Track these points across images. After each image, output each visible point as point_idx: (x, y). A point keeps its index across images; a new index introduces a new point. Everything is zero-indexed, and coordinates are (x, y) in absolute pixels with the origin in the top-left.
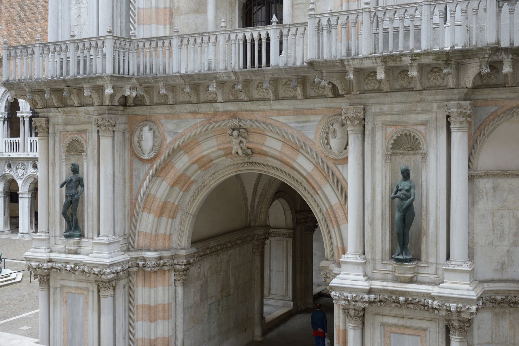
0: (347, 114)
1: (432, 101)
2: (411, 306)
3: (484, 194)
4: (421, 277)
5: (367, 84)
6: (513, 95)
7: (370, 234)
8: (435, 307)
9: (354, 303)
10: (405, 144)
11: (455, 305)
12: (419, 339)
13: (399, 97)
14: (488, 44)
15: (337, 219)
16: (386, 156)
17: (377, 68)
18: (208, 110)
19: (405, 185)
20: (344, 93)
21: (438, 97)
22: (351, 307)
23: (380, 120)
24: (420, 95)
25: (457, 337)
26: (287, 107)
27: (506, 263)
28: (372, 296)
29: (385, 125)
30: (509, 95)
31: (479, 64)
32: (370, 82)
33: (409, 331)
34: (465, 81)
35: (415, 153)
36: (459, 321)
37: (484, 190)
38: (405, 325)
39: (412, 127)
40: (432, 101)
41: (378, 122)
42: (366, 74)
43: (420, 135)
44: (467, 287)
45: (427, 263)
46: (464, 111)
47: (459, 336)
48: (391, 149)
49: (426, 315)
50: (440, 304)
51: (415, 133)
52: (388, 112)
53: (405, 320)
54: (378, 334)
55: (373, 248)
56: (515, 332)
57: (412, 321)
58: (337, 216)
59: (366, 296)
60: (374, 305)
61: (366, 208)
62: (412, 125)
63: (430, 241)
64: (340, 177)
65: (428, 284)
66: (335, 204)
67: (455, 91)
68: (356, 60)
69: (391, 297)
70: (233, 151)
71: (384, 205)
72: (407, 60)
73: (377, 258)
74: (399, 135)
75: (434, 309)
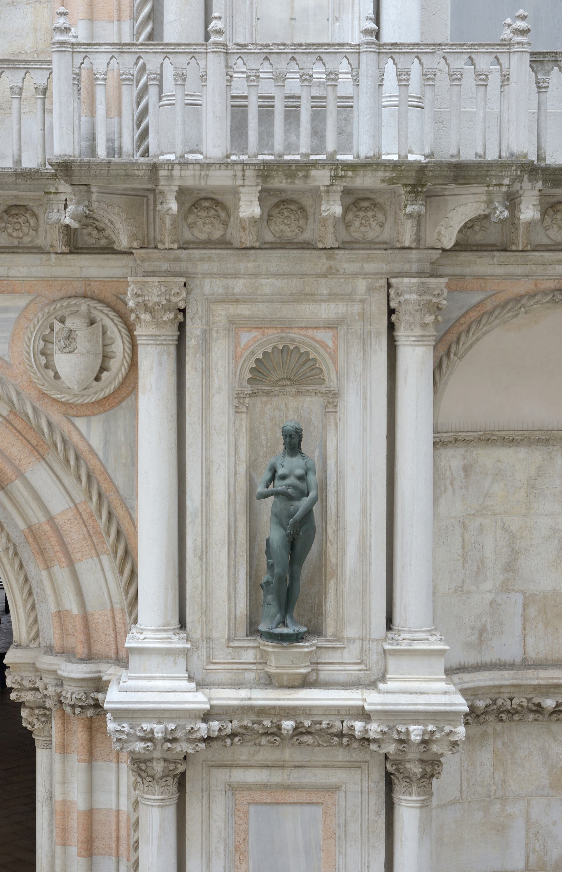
0: (142, 296)
1: (355, 275)
2: (308, 739)
3: (448, 483)
4: (326, 672)
5: (191, 226)
6: (519, 270)
7: (199, 581)
8: (372, 735)
9: (169, 745)
10: (283, 369)
11: (421, 727)
12: (318, 811)
13: (275, 260)
14: (512, 154)
15: (66, 548)
16: (239, 399)
17: (241, 189)
19: (291, 465)
20: (135, 245)
21: (370, 267)
22: (157, 754)
23: (223, 313)
24: (327, 259)
25: (414, 798)
27: (488, 628)
28: (215, 725)
29: (235, 325)
30: (511, 269)
31: (484, 198)
32: (200, 222)
33: (295, 797)
34: (439, 233)
35: (299, 393)
36: (422, 761)
37: (448, 474)
38: (287, 782)
39: (303, 332)
40: (355, 275)
41: (218, 319)
42: (203, 203)
43: (322, 351)
44: (442, 686)
45: (338, 640)
46: (434, 300)
47: (419, 795)
48: (250, 381)
49: (341, 755)
50: (386, 729)
51: (310, 346)
53: (287, 771)
54: (219, 809)
55: (206, 611)
56: (505, 773)
57: (303, 771)
58: (67, 540)
59: (203, 726)
60: (216, 745)
61: (188, 520)
62: (302, 328)
63: (346, 589)
64: (82, 446)
65: (346, 685)
66: (62, 513)
67: (414, 255)
68: (191, 167)
69: (260, 723)
71: (232, 513)
72: (321, 177)
73: (215, 635)
74: (270, 350)
75: (366, 740)
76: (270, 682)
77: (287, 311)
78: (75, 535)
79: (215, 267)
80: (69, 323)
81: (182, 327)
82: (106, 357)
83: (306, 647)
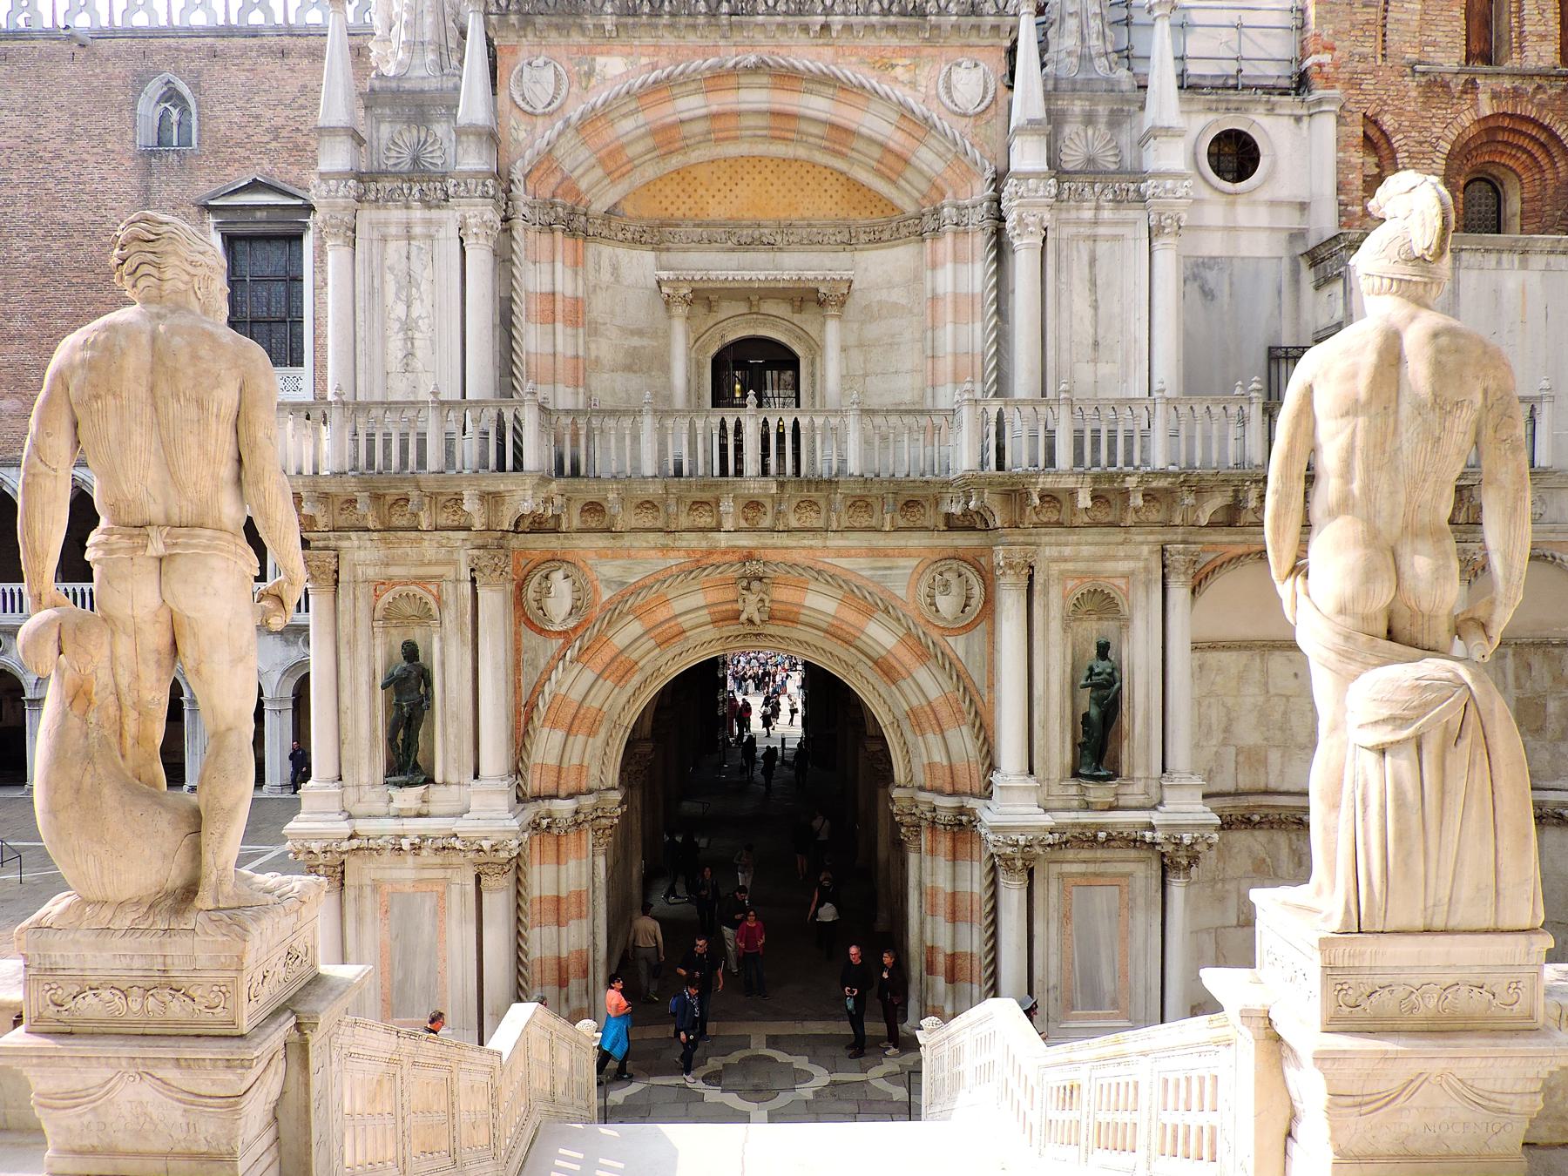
1: (1142, 543)
18: (694, 544)
19: (1101, 666)
21: (1151, 538)
26: (855, 543)
52: (1068, 557)
55: (1046, 761)
70: (744, 617)
76: (1088, 807)
77: (1098, 566)
78: (944, 713)
79: (1053, 539)
80: (946, 576)
81: (1031, 578)
82: (968, 598)
83: (1113, 784)
